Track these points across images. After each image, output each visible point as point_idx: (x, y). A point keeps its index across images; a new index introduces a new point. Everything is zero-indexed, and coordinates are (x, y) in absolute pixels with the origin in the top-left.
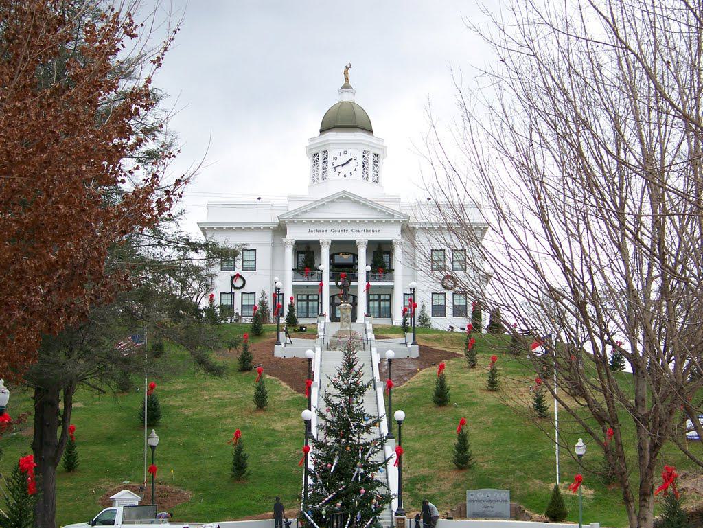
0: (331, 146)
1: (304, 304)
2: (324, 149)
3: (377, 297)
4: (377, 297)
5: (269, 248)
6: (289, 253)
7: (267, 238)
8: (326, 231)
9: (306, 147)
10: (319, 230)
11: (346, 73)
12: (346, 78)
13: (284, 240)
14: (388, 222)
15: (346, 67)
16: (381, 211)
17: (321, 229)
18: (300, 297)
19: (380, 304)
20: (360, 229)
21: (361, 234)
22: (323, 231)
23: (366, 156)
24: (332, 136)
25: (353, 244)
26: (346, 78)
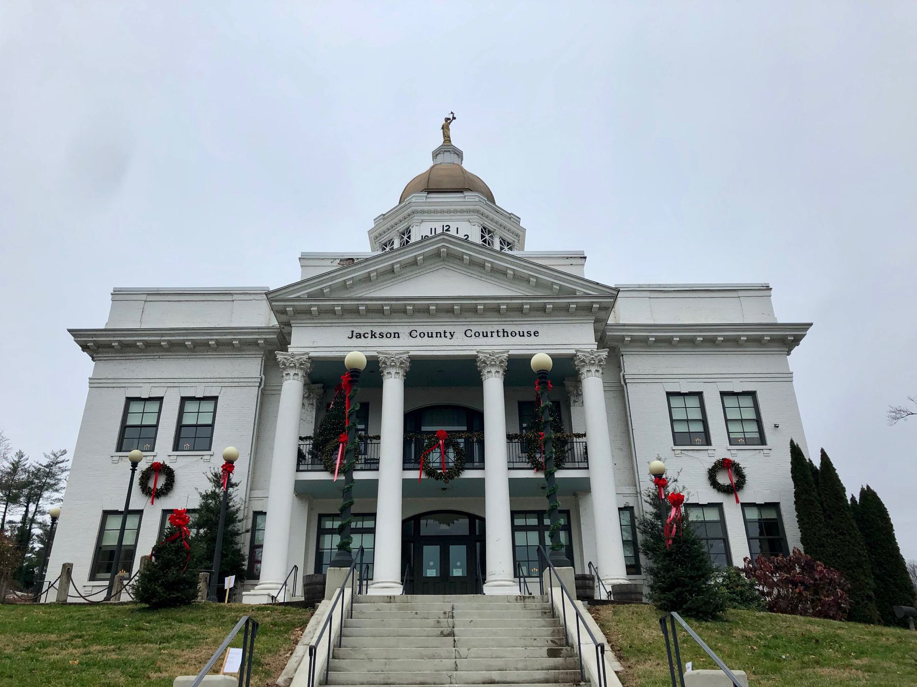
0: (417, 218)
1: (337, 539)
2: (402, 227)
3: (533, 521)
4: (533, 521)
5: (254, 392)
6: (292, 389)
7: (252, 367)
8: (397, 335)
9: (370, 232)
10: (377, 330)
11: (445, 128)
12: (447, 138)
13: (280, 356)
14: (564, 311)
15: (447, 119)
16: (539, 284)
17: (385, 330)
18: (328, 525)
19: (542, 539)
20: (489, 329)
21: (489, 340)
22: (389, 335)
23: (487, 237)
24: (419, 198)
25: (467, 372)
26: (447, 138)
